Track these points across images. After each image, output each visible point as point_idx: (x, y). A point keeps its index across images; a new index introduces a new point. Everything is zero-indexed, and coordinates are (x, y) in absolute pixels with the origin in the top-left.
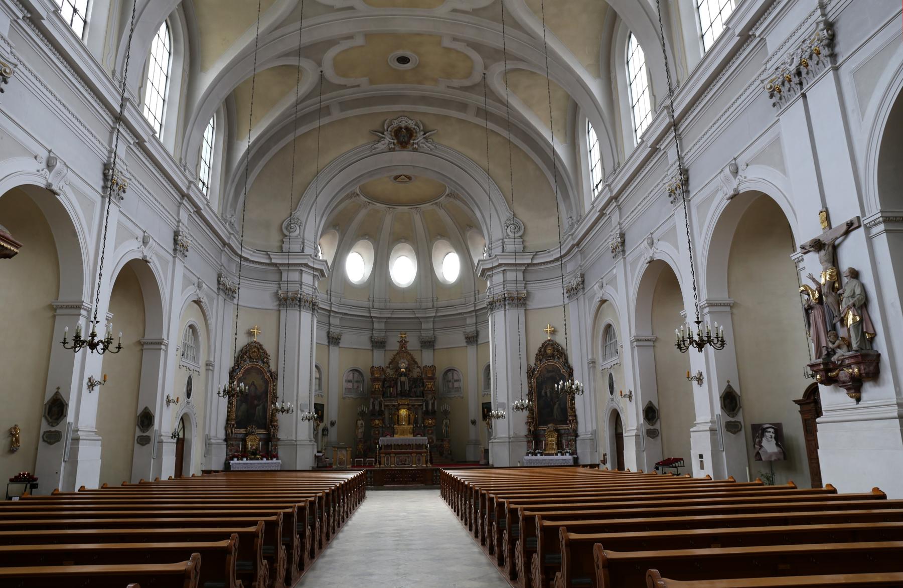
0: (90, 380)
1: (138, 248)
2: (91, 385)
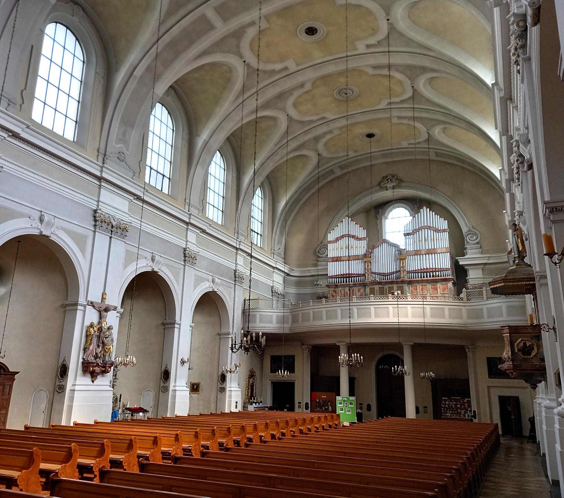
0: (182, 360)
1: (209, 286)
2: (183, 362)
